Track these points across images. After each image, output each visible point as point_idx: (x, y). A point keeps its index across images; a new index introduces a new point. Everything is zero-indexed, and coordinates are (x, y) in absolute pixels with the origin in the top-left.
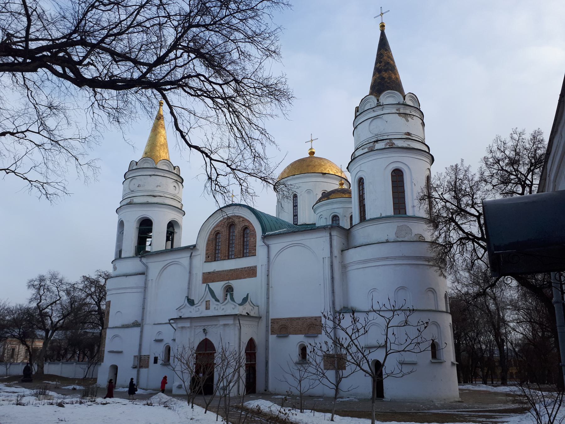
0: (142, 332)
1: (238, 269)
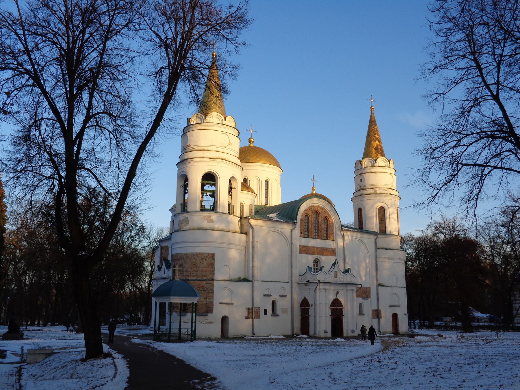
0: (253, 287)
1: (324, 248)
